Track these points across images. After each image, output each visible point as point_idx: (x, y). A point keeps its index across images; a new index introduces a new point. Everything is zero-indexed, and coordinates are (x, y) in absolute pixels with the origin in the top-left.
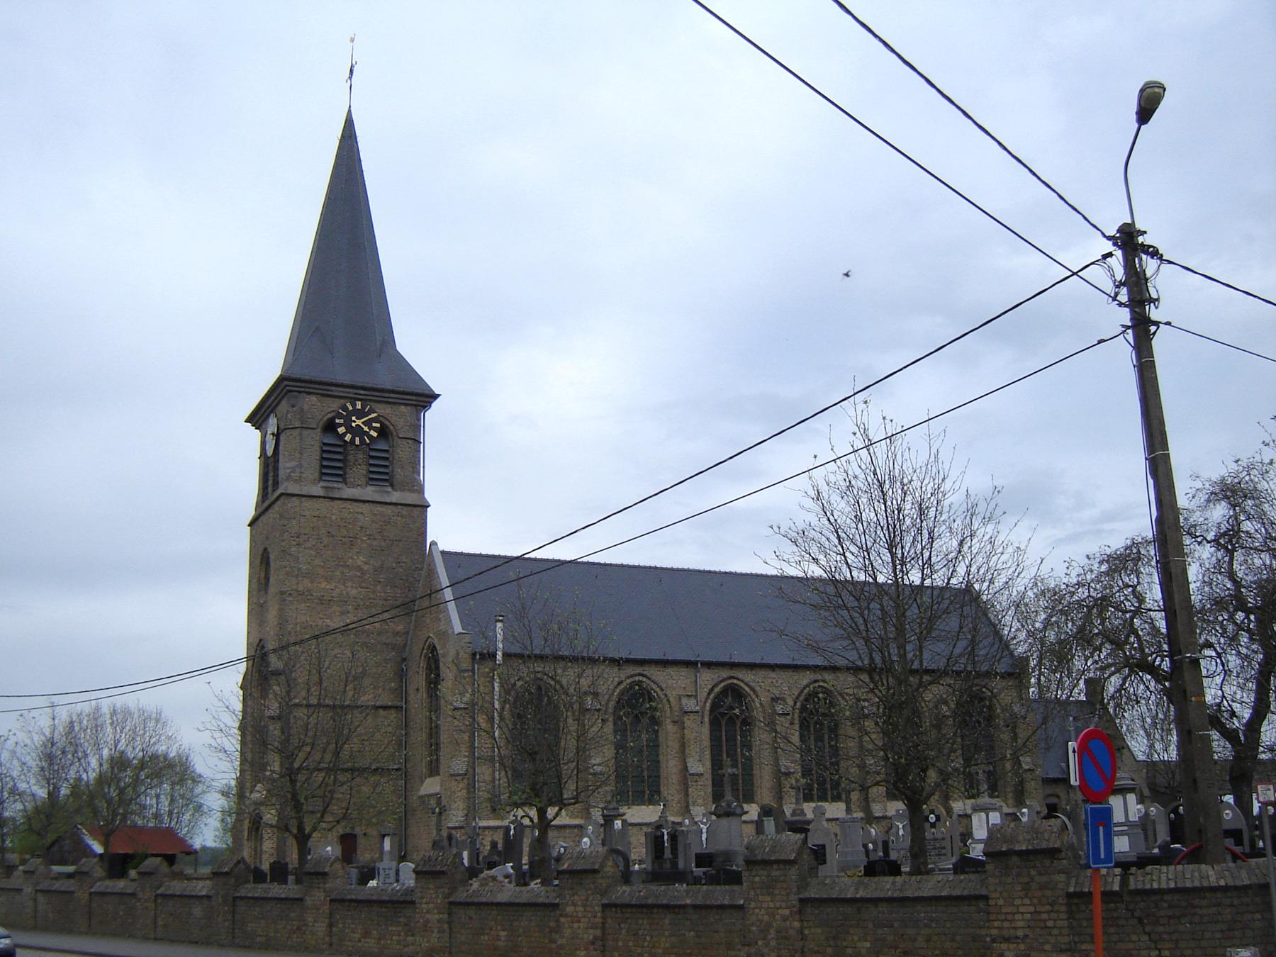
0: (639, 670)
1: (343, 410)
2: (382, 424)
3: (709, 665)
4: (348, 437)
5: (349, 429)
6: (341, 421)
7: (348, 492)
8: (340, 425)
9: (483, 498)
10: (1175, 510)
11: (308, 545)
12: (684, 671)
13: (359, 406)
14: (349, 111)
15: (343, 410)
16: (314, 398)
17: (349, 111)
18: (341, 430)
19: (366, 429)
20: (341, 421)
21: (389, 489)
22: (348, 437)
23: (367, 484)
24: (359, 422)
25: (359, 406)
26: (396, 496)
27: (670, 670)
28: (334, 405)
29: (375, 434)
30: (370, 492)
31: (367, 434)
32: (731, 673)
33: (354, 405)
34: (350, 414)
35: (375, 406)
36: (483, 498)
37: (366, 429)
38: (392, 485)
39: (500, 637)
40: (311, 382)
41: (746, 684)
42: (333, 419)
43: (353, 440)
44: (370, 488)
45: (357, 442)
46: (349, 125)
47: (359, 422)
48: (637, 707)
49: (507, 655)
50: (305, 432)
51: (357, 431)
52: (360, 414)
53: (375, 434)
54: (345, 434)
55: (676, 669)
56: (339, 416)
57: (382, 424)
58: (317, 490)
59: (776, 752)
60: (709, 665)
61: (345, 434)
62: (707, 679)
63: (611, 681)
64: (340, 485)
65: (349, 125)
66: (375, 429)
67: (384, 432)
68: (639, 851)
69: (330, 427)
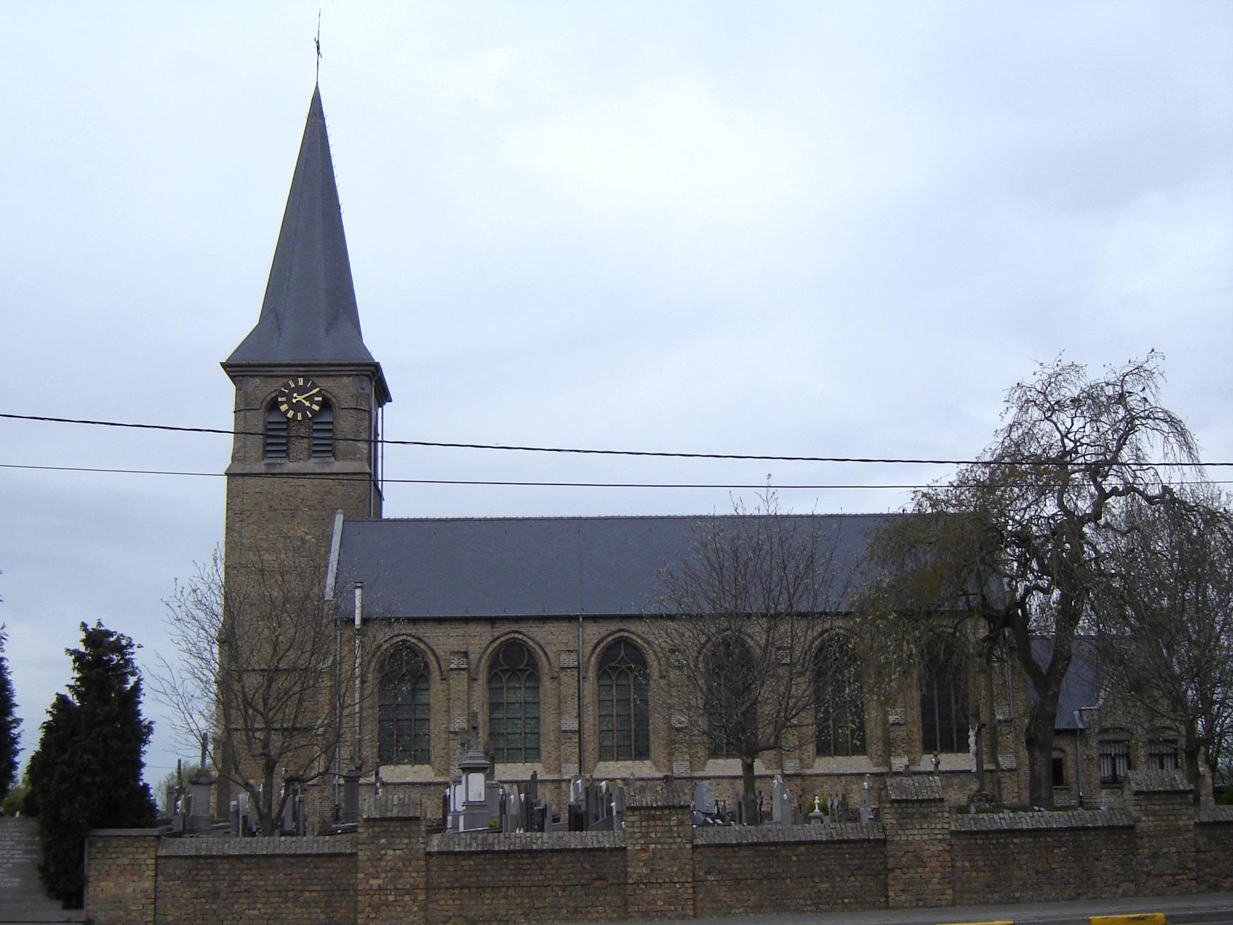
0: (515, 627)
1: (306, 385)
2: (324, 397)
3: (595, 619)
4: (290, 414)
5: (293, 406)
6: (284, 399)
7: (291, 466)
8: (283, 403)
9: (447, 454)
10: (266, 778)
11: (251, 520)
12: (565, 626)
13: (301, 383)
14: (317, 88)
15: (306, 385)
16: (257, 380)
17: (317, 88)
18: (284, 408)
19: (307, 404)
20: (284, 399)
21: (332, 460)
22: (290, 414)
23: (310, 457)
24: (299, 398)
25: (301, 383)
26: (336, 466)
27: (550, 627)
28: (277, 384)
29: (316, 408)
30: (312, 465)
31: (310, 409)
32: (621, 626)
33: (296, 382)
34: (293, 391)
35: (316, 380)
36: (447, 454)
37: (307, 404)
38: (334, 456)
39: (358, 604)
40: (250, 366)
41: (639, 636)
42: (276, 397)
43: (295, 416)
44: (313, 460)
45: (299, 417)
46: (316, 101)
47: (299, 398)
48: (513, 664)
49: (365, 621)
50: (249, 413)
51: (298, 407)
52: (301, 390)
53: (316, 408)
54: (287, 411)
55: (556, 624)
56: (282, 394)
57: (324, 397)
58: (260, 468)
59: (673, 701)
60: (595, 619)
61: (287, 411)
62: (593, 632)
63: (480, 640)
64: (283, 461)
65: (316, 101)
66: (317, 403)
67: (326, 405)
68: (515, 798)
69: (274, 406)
